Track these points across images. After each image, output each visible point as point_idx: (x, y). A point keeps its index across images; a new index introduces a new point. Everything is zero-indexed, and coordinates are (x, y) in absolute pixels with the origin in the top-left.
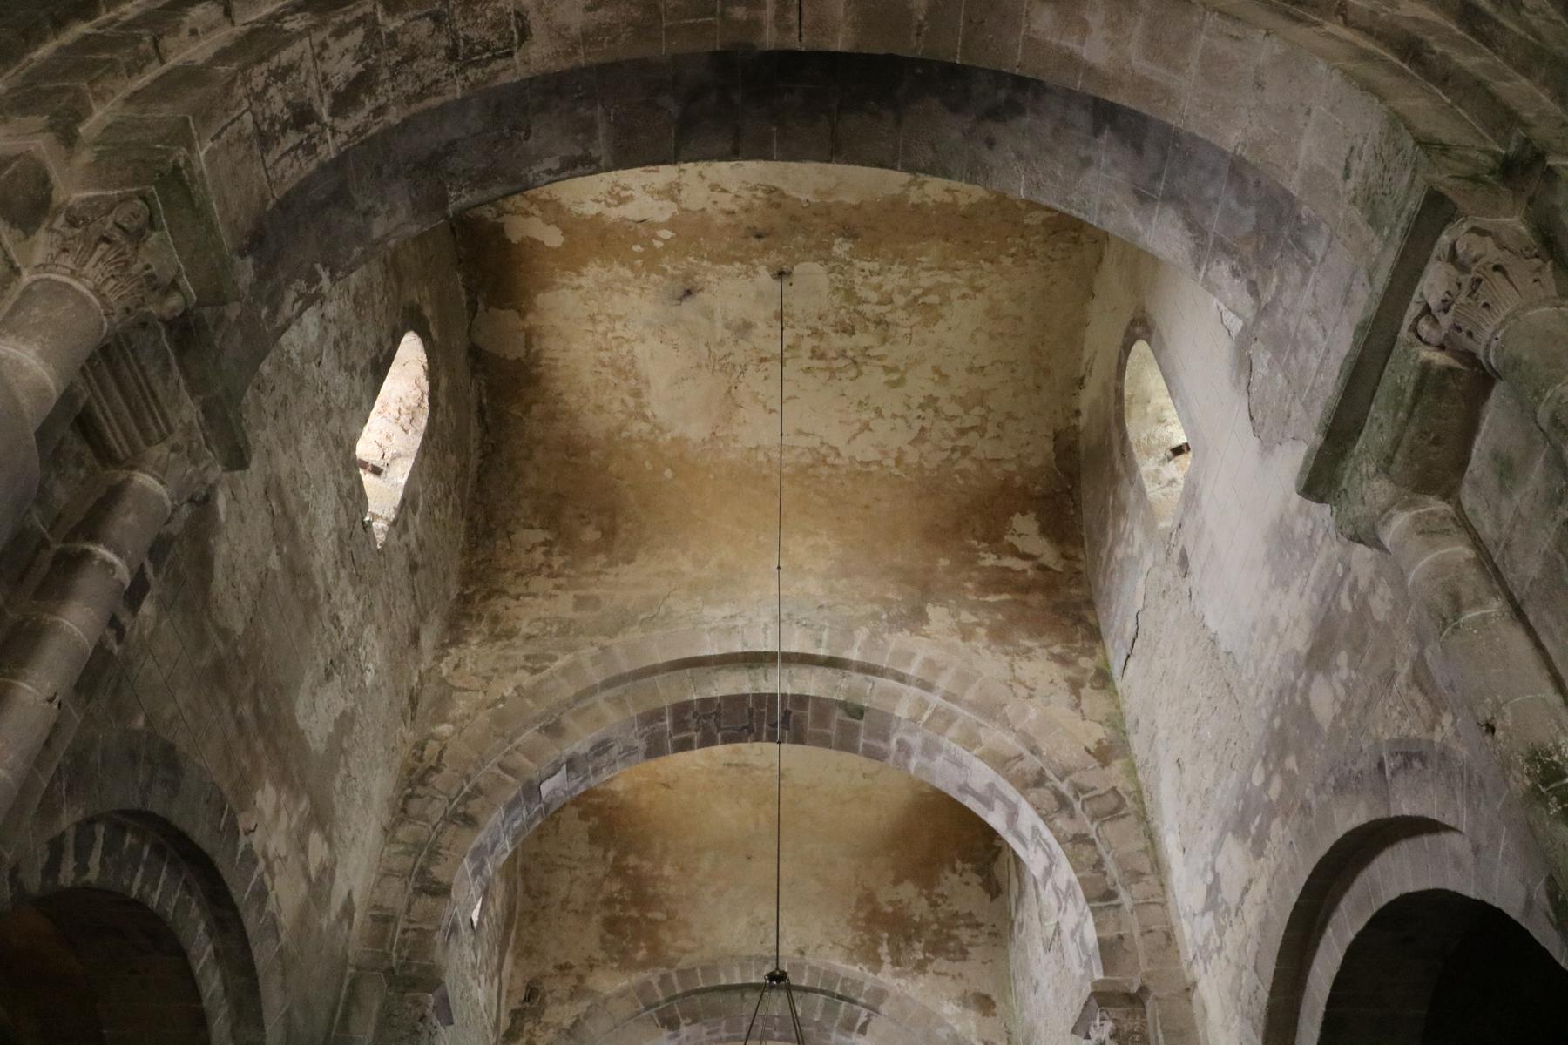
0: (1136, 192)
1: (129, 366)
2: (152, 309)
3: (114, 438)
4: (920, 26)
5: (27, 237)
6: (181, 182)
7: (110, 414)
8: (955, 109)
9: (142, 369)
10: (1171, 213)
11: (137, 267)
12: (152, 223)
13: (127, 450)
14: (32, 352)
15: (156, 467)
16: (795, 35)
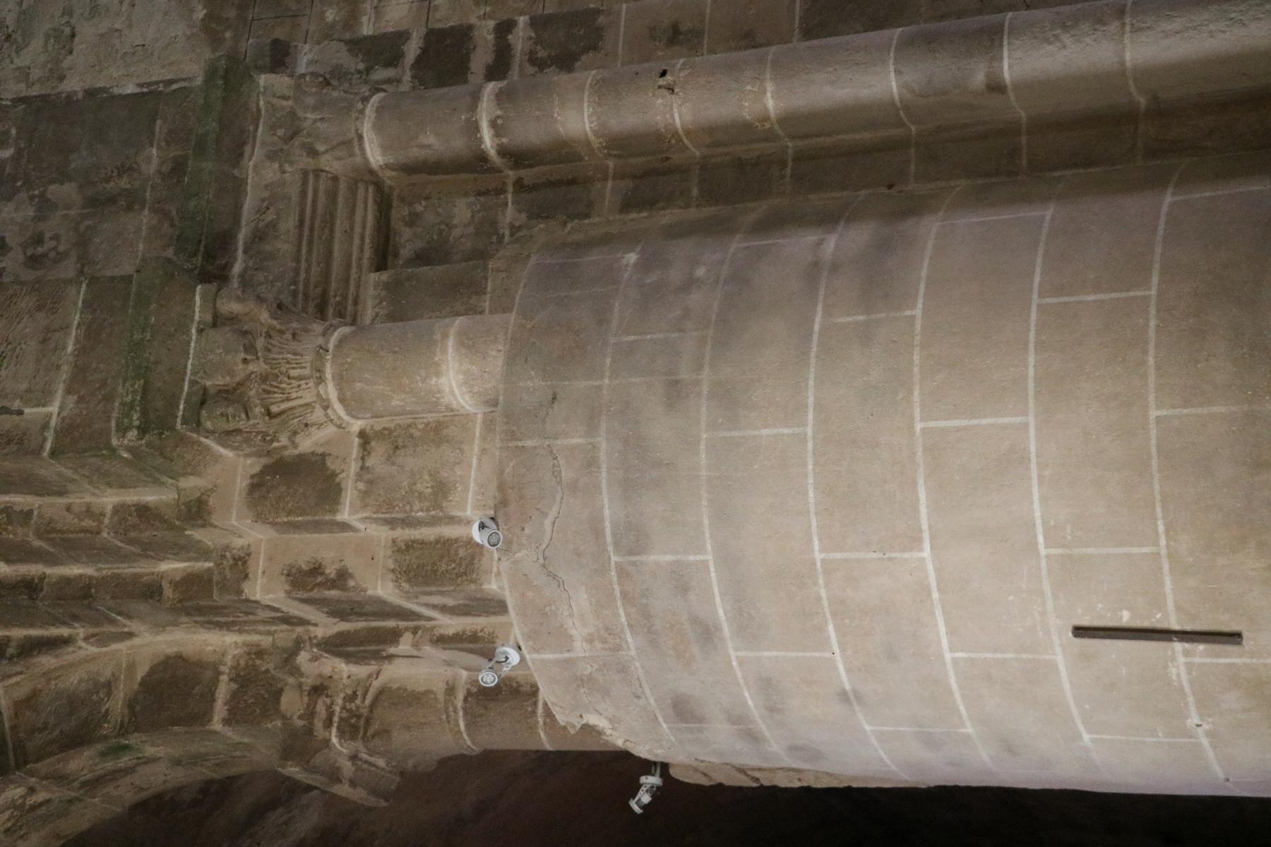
1: (308, 271)
2: (264, 316)
3: (367, 215)
5: (323, 455)
6: (144, 413)
7: (357, 241)
9: (298, 261)
11: (259, 367)
12: (203, 399)
13: (361, 192)
14: (443, 380)
15: (352, 155)
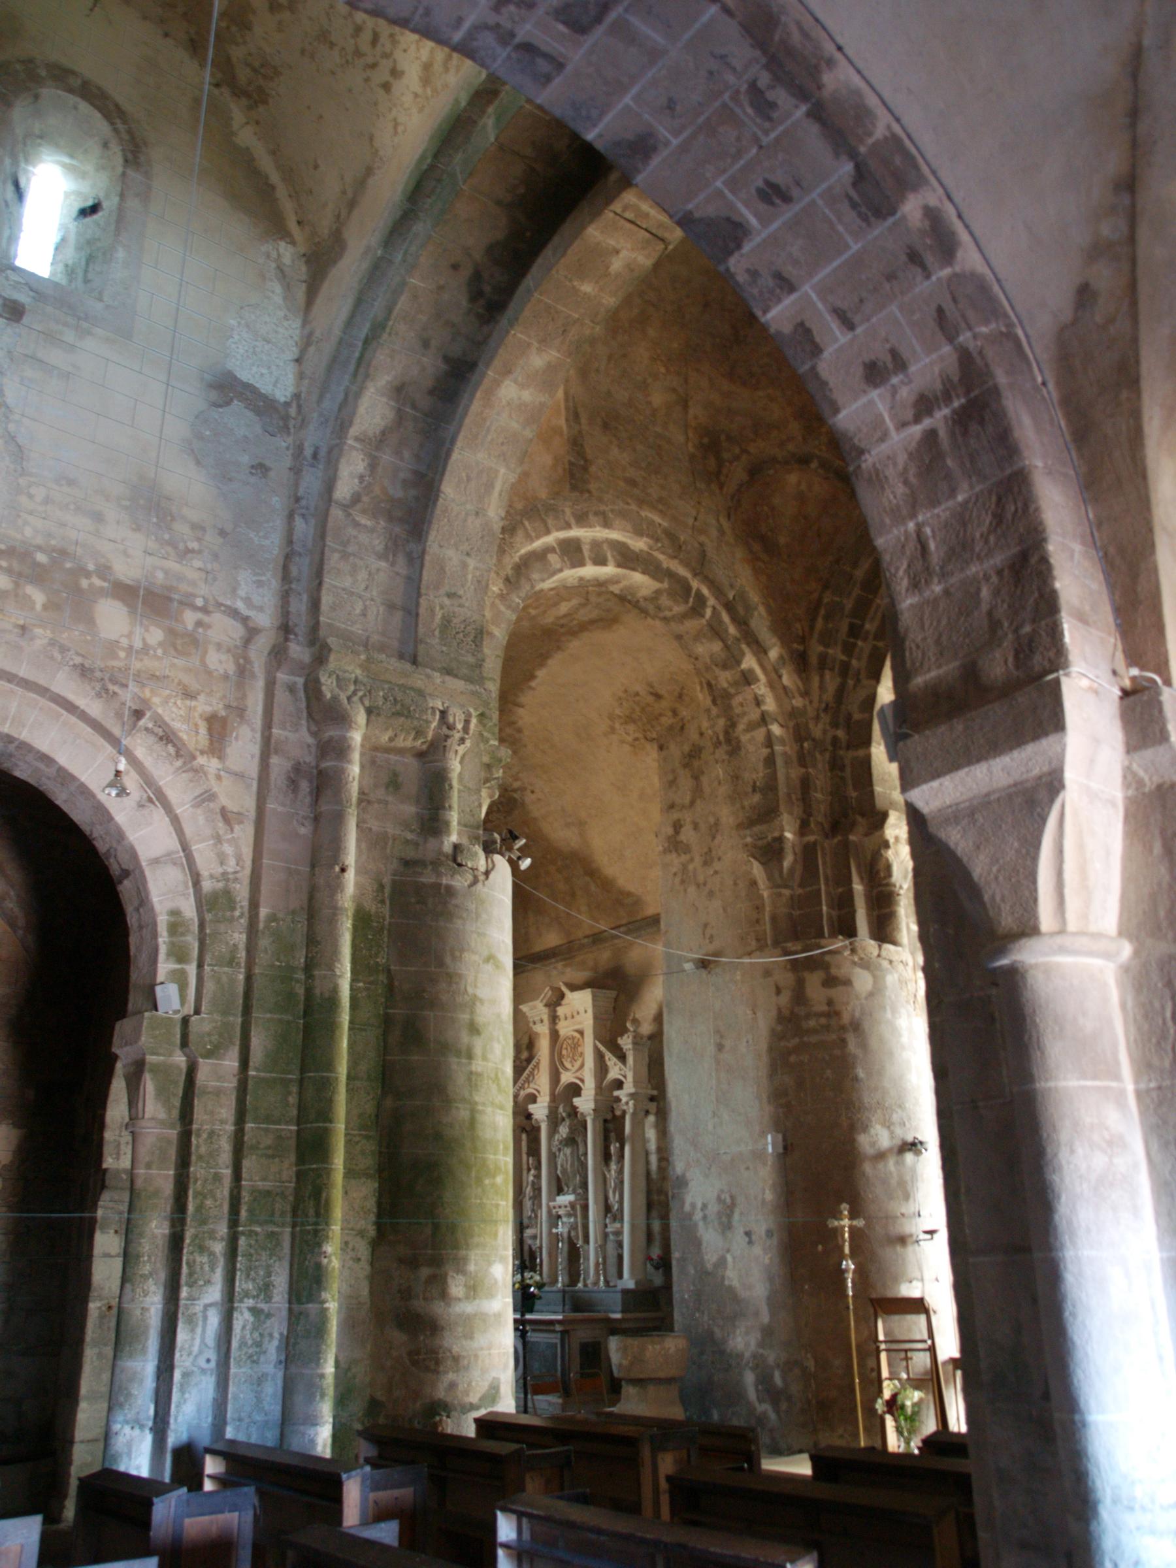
0: (403, 385)
4: (570, 280)
8: (490, 249)
10: (391, 415)
16: (619, 211)
